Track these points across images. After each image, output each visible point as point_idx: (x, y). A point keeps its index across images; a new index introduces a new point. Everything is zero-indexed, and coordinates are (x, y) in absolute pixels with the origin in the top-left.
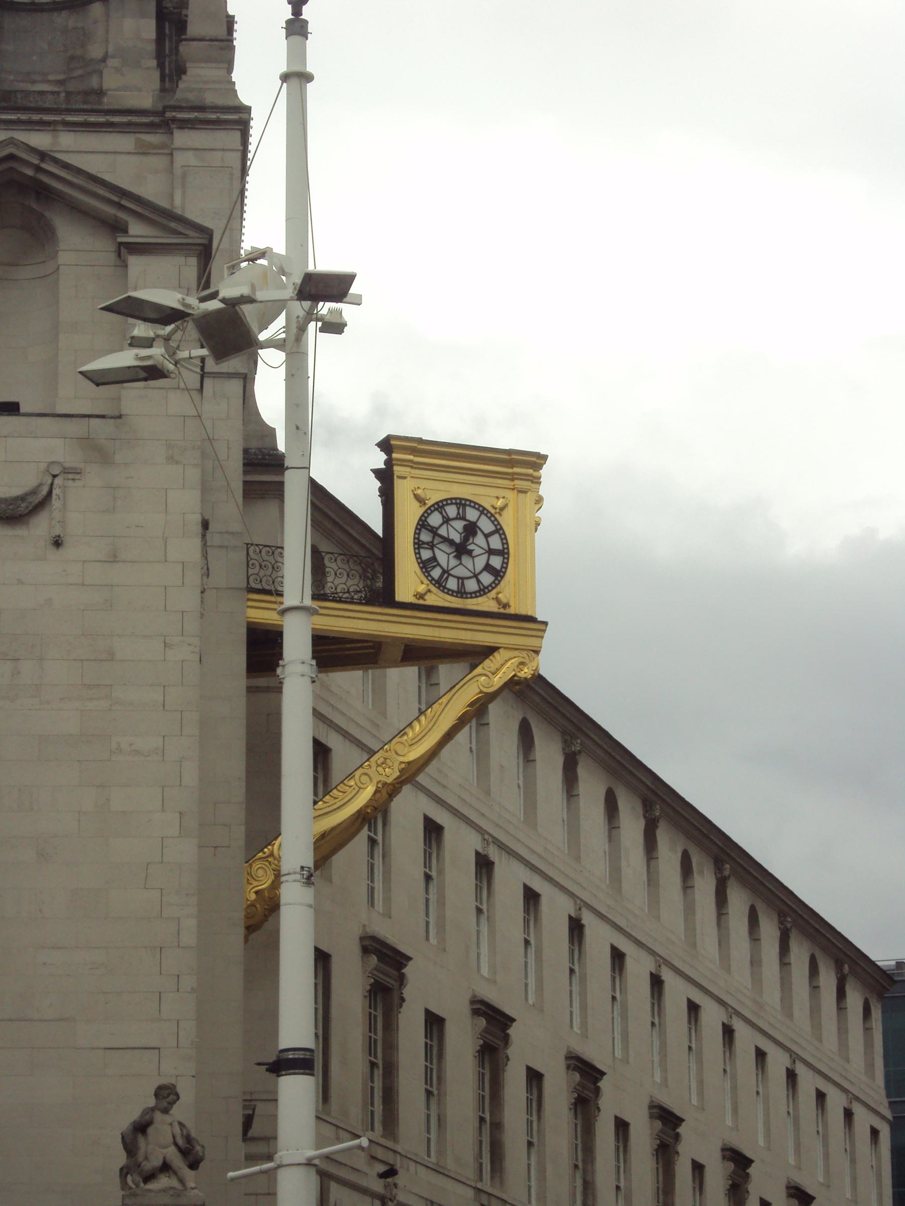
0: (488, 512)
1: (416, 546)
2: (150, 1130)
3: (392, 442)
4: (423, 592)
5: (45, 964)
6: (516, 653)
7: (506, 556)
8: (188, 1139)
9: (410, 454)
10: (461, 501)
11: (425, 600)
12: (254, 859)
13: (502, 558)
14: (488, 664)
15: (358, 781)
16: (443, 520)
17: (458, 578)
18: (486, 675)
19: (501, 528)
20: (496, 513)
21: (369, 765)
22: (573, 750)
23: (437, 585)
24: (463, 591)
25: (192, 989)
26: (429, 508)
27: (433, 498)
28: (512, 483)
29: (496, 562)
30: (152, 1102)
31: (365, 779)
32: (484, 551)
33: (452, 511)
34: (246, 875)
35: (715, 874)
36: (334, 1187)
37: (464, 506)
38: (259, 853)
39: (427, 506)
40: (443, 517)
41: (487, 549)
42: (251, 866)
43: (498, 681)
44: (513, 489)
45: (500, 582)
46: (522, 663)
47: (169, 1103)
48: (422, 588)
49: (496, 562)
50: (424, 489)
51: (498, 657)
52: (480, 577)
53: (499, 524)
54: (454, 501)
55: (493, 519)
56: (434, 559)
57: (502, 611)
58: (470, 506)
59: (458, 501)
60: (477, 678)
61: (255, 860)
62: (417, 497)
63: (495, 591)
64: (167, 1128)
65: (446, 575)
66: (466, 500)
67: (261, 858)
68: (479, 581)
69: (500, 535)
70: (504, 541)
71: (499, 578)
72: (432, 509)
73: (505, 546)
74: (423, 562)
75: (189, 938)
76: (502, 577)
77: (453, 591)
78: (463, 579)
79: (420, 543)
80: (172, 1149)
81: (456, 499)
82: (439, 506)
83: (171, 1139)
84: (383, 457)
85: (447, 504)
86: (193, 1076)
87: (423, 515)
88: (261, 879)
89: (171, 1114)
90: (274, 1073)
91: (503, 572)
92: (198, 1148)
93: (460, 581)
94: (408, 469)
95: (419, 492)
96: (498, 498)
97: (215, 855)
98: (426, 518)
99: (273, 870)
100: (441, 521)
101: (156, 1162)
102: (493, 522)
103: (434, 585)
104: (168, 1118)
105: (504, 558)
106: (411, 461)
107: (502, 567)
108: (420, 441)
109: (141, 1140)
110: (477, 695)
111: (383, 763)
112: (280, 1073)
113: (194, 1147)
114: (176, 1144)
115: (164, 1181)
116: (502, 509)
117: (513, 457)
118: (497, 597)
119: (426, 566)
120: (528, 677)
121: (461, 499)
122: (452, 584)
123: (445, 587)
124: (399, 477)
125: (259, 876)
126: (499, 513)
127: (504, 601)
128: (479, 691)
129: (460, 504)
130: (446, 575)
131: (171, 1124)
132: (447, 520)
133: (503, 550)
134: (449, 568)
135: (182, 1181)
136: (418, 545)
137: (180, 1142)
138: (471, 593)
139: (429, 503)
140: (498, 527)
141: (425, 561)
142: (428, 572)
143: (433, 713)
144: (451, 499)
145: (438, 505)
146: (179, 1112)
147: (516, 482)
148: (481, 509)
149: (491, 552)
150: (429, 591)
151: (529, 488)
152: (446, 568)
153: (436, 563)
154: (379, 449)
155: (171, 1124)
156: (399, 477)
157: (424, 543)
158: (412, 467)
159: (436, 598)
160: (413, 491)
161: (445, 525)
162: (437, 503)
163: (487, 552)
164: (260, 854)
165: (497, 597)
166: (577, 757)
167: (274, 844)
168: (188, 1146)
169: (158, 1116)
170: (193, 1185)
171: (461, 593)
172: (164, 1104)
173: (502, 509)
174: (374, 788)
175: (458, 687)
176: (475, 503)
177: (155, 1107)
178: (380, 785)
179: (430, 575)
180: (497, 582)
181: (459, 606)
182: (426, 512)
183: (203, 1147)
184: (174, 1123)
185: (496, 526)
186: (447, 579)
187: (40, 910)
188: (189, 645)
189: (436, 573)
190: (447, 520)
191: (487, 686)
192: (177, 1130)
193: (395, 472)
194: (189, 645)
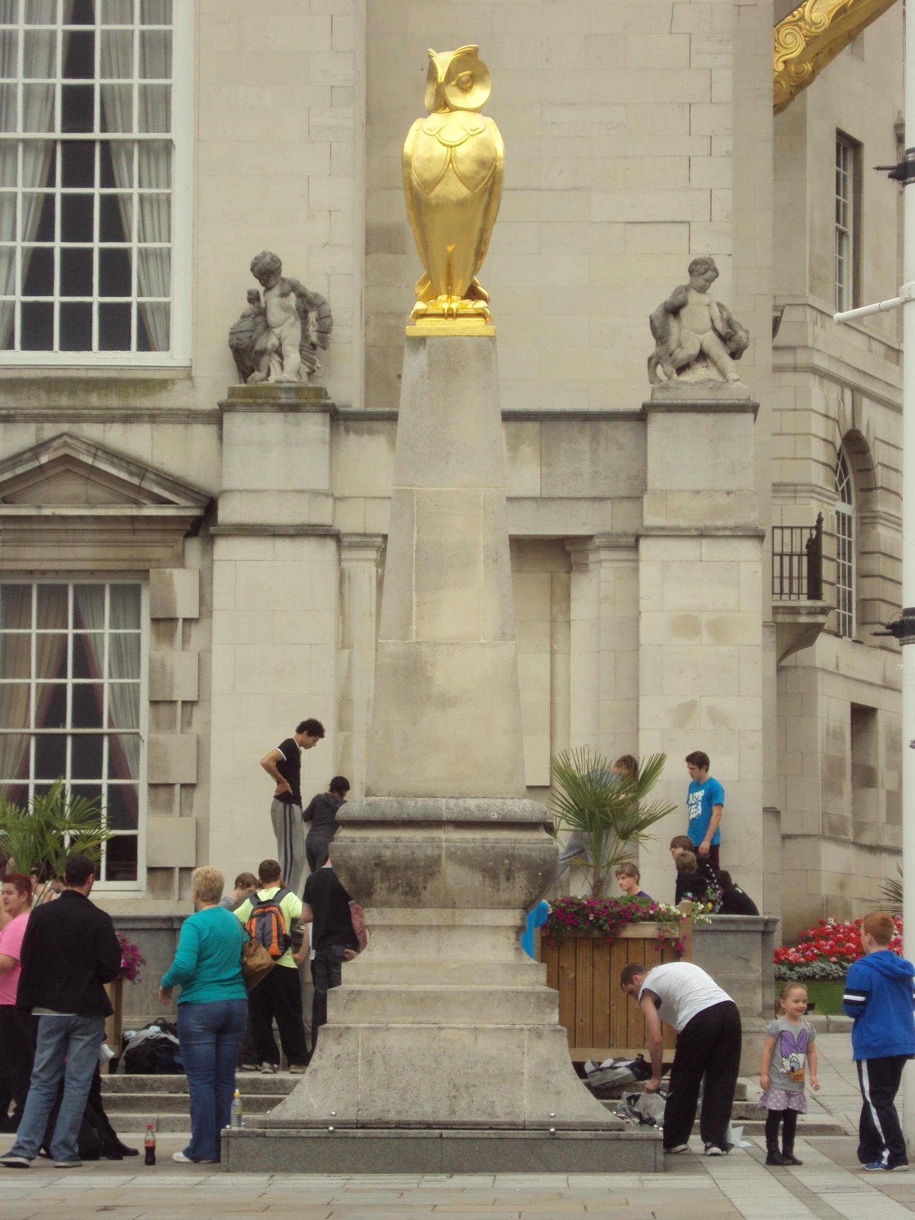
2: (684, 312)
5: (553, 123)
8: (729, 323)
12: (783, 22)
25: (727, 152)
30: (685, 280)
34: (773, 42)
36: (867, 406)
38: (787, 16)
42: (778, 31)
47: (707, 281)
61: (784, 24)
64: (705, 311)
67: (790, 22)
75: (723, 93)
80: (711, 335)
83: (709, 324)
86: (730, 255)
88: (789, 46)
89: (708, 294)
90: (898, 179)
92: (741, 333)
97: (739, 15)
99: (804, 36)
101: (694, 351)
104: (705, 299)
109: (673, 324)
112: (908, 180)
113: (736, 332)
114: (715, 329)
115: (700, 372)
125: (788, 42)
131: (709, 305)
135: (721, 372)
137: (720, 326)
146: (720, 290)
155: (709, 305)
164: (789, 18)
167: (805, 6)
168: (729, 330)
169: (693, 296)
170: (735, 377)
172: (701, 281)
177: (689, 285)
183: (747, 332)
184: (712, 304)
187: (547, 60)
192: (716, 312)
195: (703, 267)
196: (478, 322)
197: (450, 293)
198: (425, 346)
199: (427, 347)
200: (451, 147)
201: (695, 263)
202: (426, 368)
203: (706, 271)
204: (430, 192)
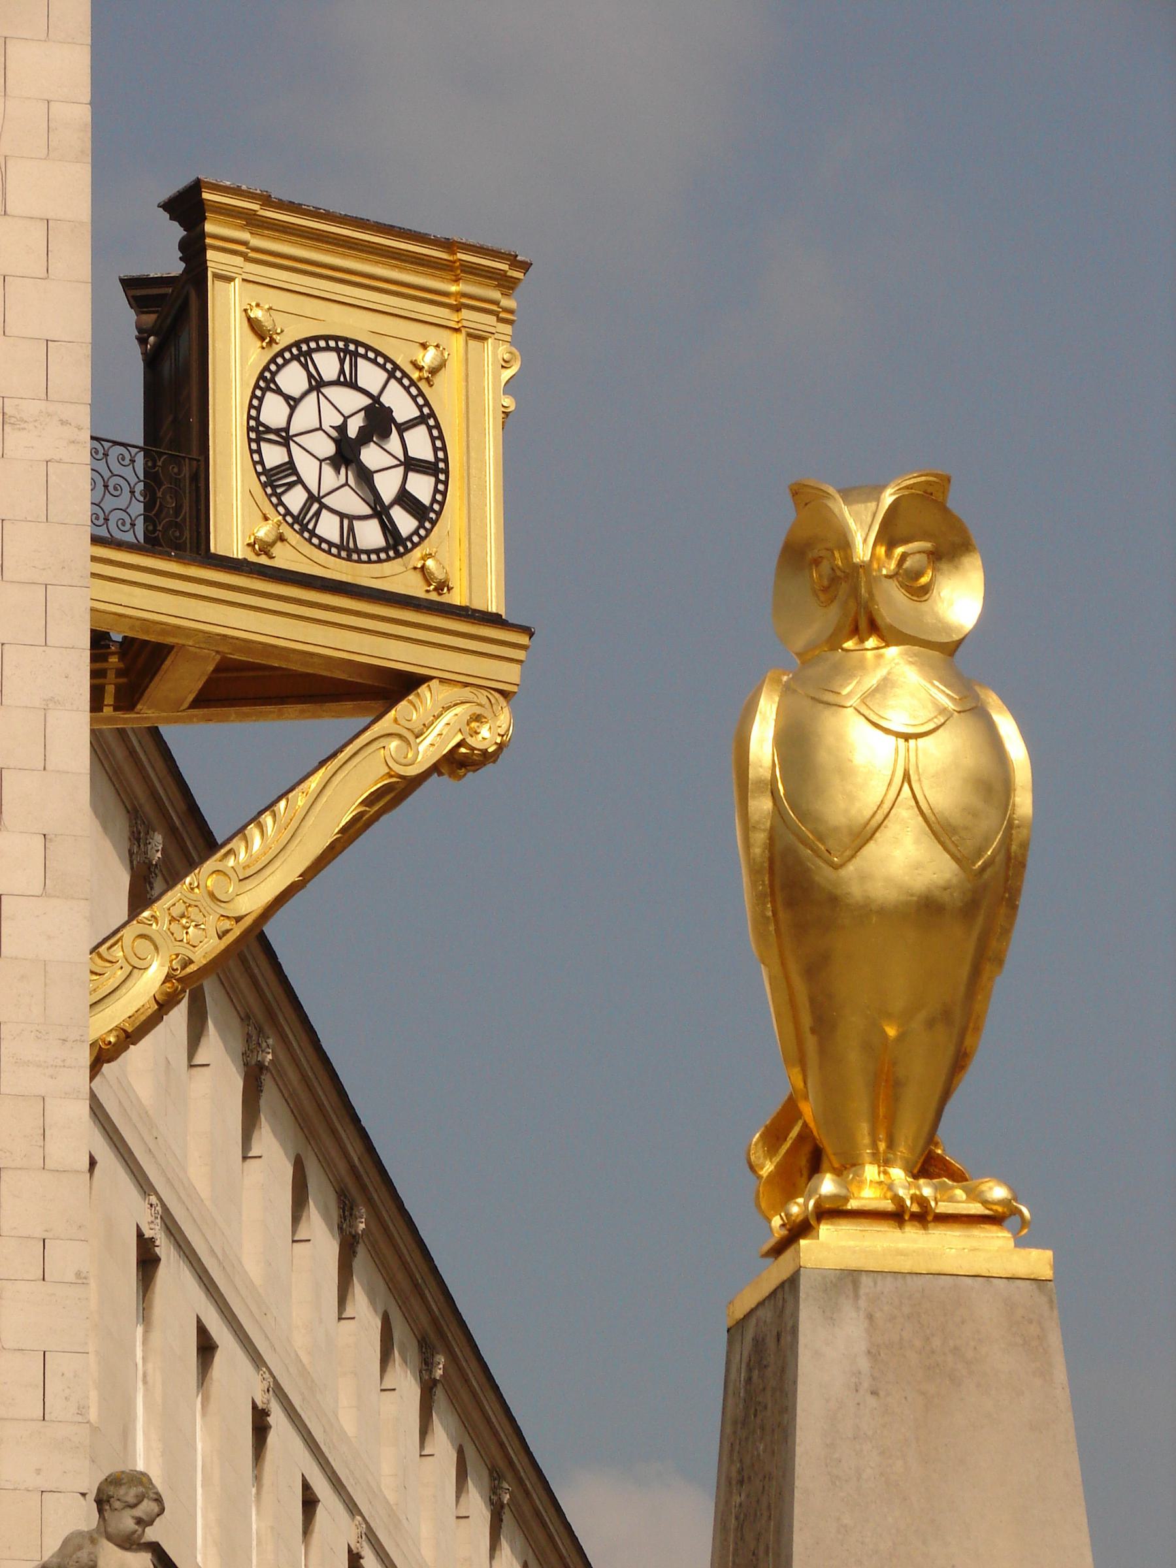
0: (405, 375)
1: (253, 435)
3: (206, 196)
4: (270, 539)
6: (466, 693)
7: (442, 477)
9: (242, 227)
10: (346, 346)
11: (272, 557)
13: (433, 479)
14: (406, 712)
15: (128, 950)
16: (310, 382)
17: (342, 516)
18: (400, 736)
19: (432, 414)
20: (420, 379)
21: (152, 916)
22: (259, 1059)
23: (297, 527)
24: (351, 545)
26: (280, 354)
28: (455, 317)
29: (421, 487)
31: (144, 946)
32: (397, 462)
33: (328, 364)
35: (420, 1372)
37: (355, 354)
39: (276, 348)
40: (310, 376)
41: (403, 459)
43: (427, 751)
44: (457, 330)
45: (429, 532)
46: (478, 718)
47: (139, 1521)
48: (264, 531)
49: (421, 487)
50: (270, 308)
51: (428, 697)
53: (427, 404)
54: (332, 344)
55: (414, 391)
56: (290, 467)
57: (434, 596)
58: (365, 357)
60: (382, 743)
62: (254, 326)
63: (417, 553)
65: (316, 506)
66: (358, 343)
69: (430, 428)
70: (438, 444)
71: (427, 525)
72: (287, 355)
73: (441, 455)
74: (266, 472)
76: (434, 523)
77: (331, 544)
78: (352, 518)
79: (261, 429)
81: (337, 339)
82: (302, 352)
84: (178, 232)
85: (319, 349)
87: (266, 368)
91: (434, 511)
93: (346, 522)
94: (239, 261)
95: (257, 314)
96: (424, 346)
98: (274, 374)
100: (306, 386)
102: (414, 398)
103: (291, 526)
105: (438, 481)
106: (245, 243)
107: (434, 500)
108: (267, 201)
110: (382, 778)
111: (183, 916)
116: (434, 371)
117: (460, 256)
118: (423, 567)
120: (490, 750)
121: (347, 341)
122: (328, 527)
123: (313, 533)
124: (216, 276)
126: (427, 379)
127: (440, 575)
128: (387, 770)
129: (346, 351)
130: (316, 506)
132: (317, 384)
133: (436, 464)
134: (321, 495)
136: (258, 432)
138: (368, 552)
141: (272, 469)
142: (279, 496)
143: (290, 814)
144: (326, 338)
145: (299, 349)
147: (465, 313)
148: (389, 366)
149: (411, 464)
150: (281, 538)
151: (492, 330)
152: (315, 493)
153: (294, 478)
154: (168, 216)
156: (216, 276)
157: (269, 430)
158: (247, 259)
160: (245, 310)
161: (314, 395)
162: (297, 344)
163: (401, 464)
165: (423, 567)
166: (263, 1077)
171: (347, 549)
173: (434, 371)
174: (165, 970)
175: (342, 756)
176: (378, 353)
178: (175, 965)
179: (281, 503)
180: (383, 556)
181: (344, 578)
182: (273, 360)
185: (420, 408)
186: (317, 514)
188: (63, 422)
189: (295, 499)
190: (317, 384)
191: (404, 761)
193: (209, 264)
194: (63, 422)
195: (133, 1491)
196: (997, 1239)
197: (884, 1163)
198: (857, 1297)
199: (862, 1303)
200: (907, 737)
201: (114, 1481)
202: (864, 1364)
203: (140, 1499)
204: (842, 865)
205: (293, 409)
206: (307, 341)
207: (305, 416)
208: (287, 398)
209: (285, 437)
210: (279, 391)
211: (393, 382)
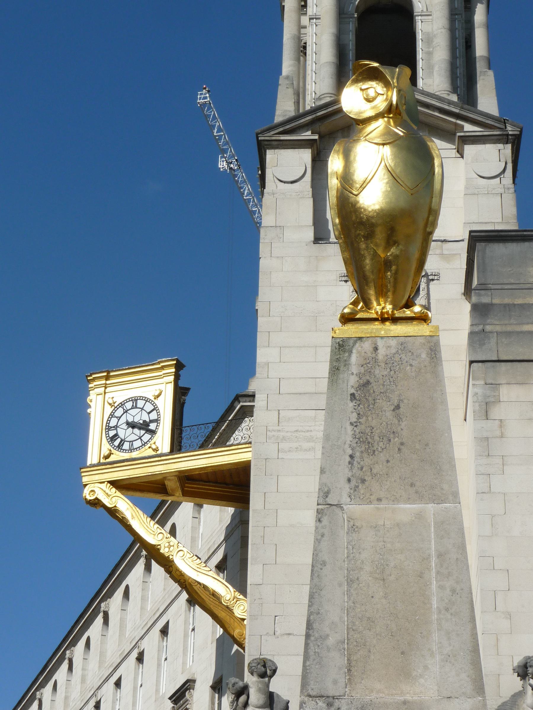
17: (130, 442)
27: (119, 401)
37: (136, 400)
40: (124, 409)
52: (142, 438)
56: (116, 435)
59: (133, 399)
68: (141, 440)
82: (122, 404)
87: (112, 412)
119: (113, 439)
139: (116, 405)
140: (156, 406)
157: (111, 427)
159: (117, 456)
162: (121, 403)
171: (131, 450)
182: (114, 410)
189: (117, 443)
205: (119, 420)
206: (123, 401)
207: (123, 420)
208: (117, 417)
209: (116, 427)
210: (115, 417)
211: (147, 402)
